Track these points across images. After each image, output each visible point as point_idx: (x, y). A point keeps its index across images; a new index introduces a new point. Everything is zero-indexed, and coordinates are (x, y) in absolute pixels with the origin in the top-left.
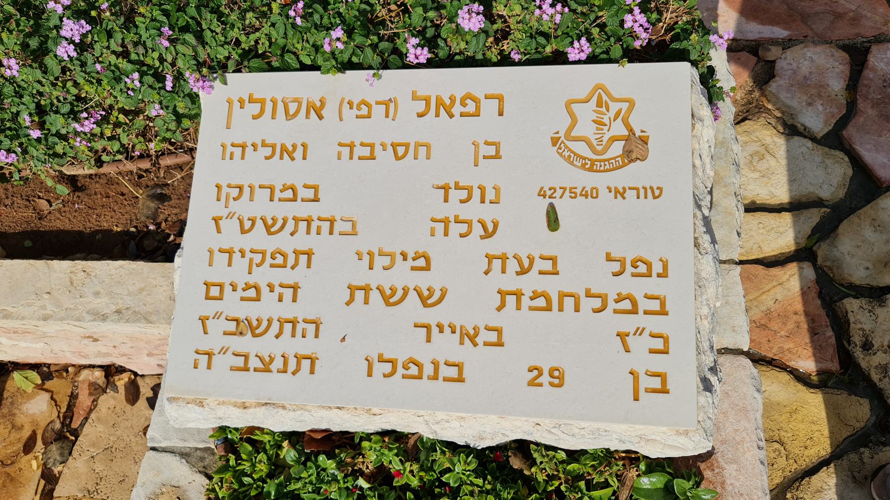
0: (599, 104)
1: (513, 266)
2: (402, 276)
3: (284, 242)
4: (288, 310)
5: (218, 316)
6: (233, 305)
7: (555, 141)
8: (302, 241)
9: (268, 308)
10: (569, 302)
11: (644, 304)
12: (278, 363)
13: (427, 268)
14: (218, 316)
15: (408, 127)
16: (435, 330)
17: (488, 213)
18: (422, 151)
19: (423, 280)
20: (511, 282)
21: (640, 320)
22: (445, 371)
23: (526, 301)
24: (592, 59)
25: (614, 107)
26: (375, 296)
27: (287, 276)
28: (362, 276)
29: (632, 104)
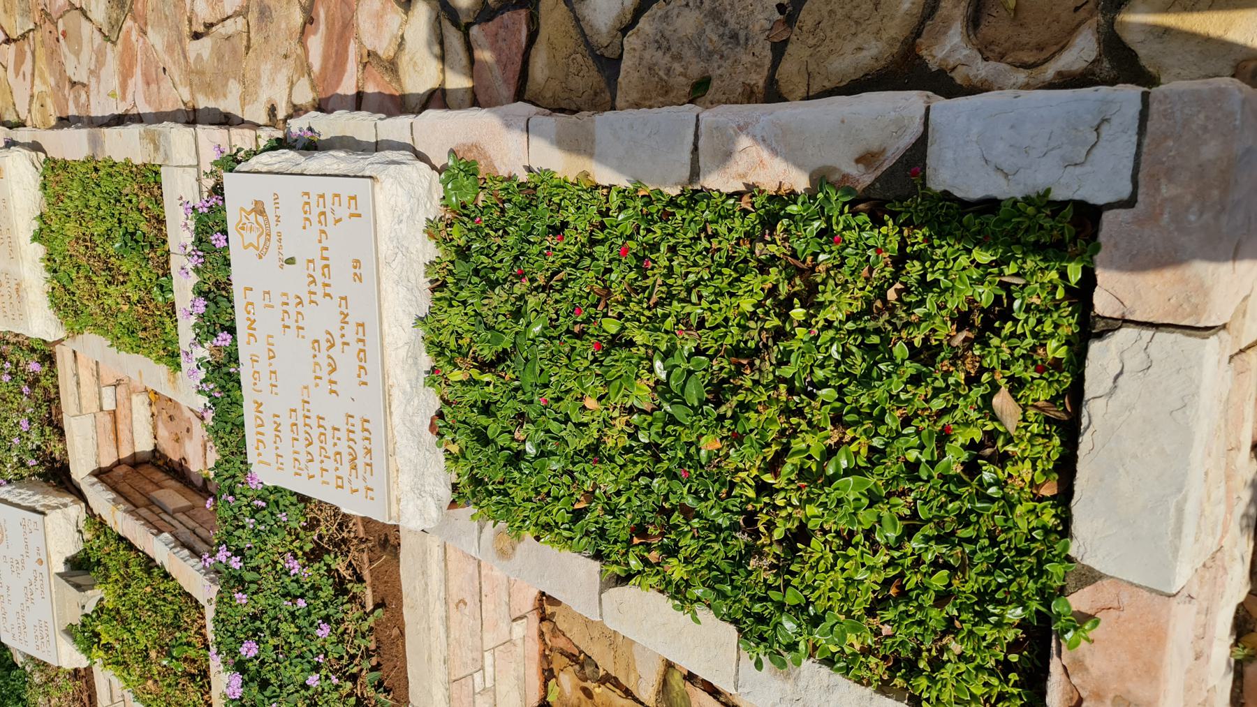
0: (243, 228)
1: (312, 287)
2: (323, 359)
3: (315, 432)
4: (343, 434)
5: (350, 482)
6: (345, 470)
7: (260, 258)
8: (313, 422)
9: (343, 447)
10: (325, 254)
11: (321, 209)
12: (367, 442)
13: (317, 341)
14: (350, 482)
15: (260, 348)
16: (345, 340)
17: (294, 301)
18: (271, 340)
19: (324, 345)
20: (319, 289)
21: (328, 211)
22: (360, 336)
23: (327, 281)
24: (224, 232)
25: (244, 220)
26: (334, 377)
27: (329, 432)
28: (324, 383)
29: (242, 209)
